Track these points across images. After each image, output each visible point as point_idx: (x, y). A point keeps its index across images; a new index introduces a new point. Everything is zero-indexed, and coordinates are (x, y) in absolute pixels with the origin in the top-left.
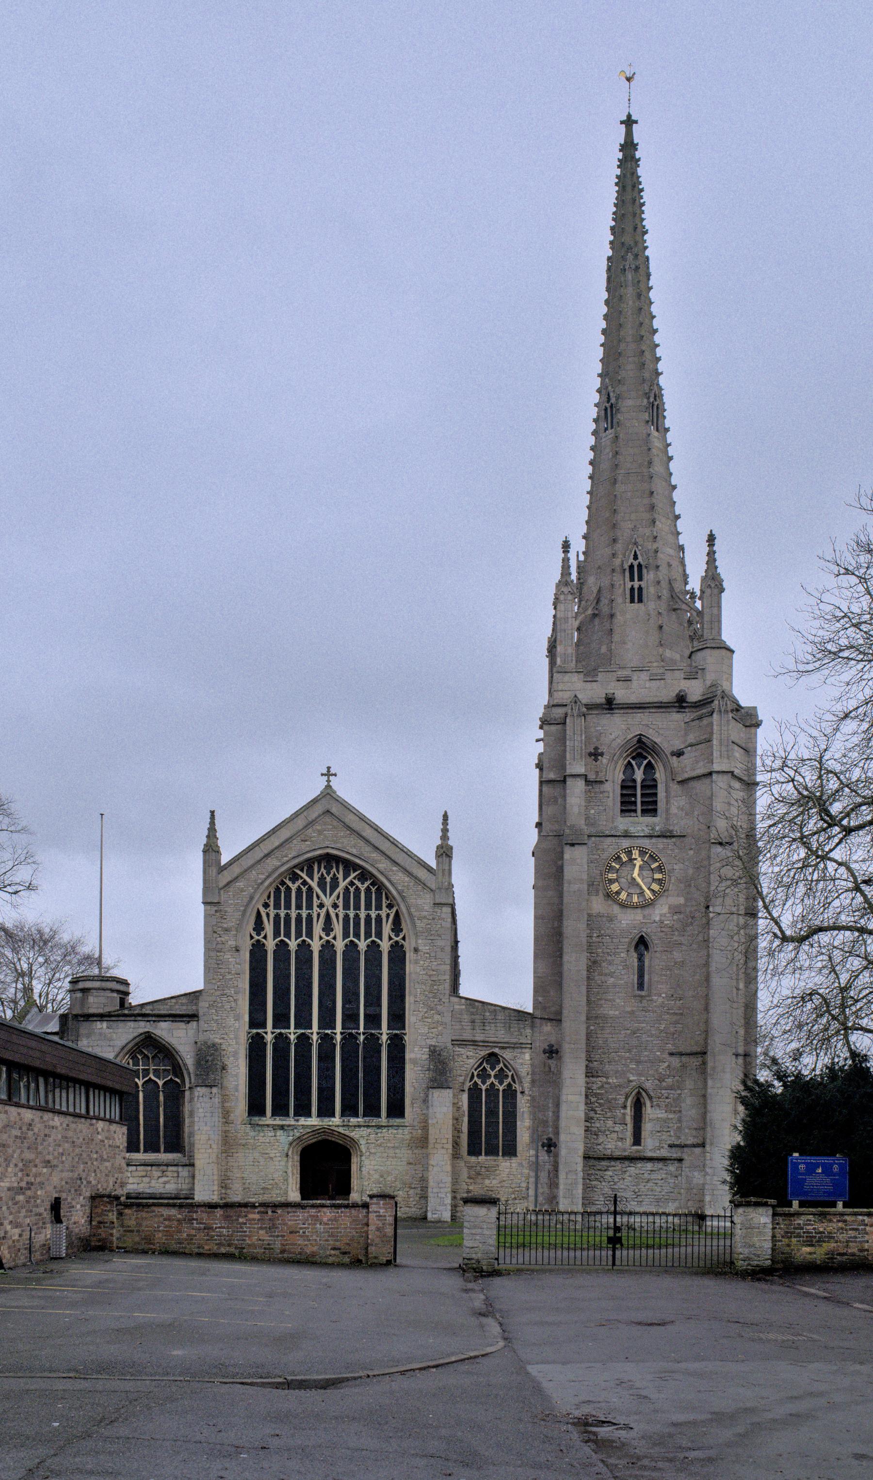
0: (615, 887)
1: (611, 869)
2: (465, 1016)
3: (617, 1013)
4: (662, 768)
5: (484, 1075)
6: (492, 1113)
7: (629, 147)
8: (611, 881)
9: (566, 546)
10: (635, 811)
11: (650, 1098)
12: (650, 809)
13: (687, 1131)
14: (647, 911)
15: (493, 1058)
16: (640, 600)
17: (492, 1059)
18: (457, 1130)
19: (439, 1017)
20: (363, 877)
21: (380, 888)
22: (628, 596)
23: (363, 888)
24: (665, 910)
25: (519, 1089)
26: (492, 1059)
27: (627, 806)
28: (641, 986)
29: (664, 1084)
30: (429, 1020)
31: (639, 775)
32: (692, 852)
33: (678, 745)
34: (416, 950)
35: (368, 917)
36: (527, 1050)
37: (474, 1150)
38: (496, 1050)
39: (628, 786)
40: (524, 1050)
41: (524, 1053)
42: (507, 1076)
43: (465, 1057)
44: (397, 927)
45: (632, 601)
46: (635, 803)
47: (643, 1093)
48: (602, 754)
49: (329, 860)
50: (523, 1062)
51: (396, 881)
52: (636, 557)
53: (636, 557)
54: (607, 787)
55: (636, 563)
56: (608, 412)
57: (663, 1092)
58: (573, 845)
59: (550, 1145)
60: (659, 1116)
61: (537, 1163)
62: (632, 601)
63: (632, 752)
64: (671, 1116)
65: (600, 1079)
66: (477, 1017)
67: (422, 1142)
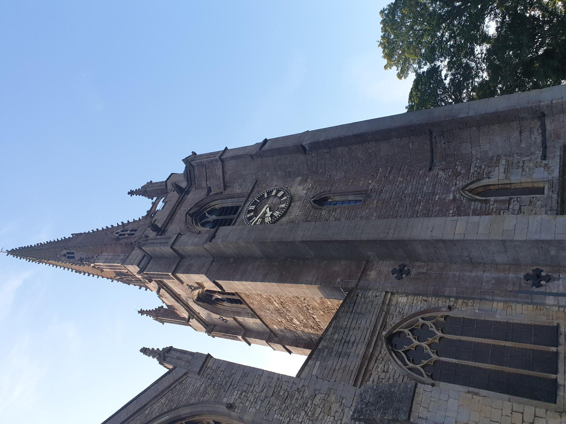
2: (330, 363)
6: (478, 353)
11: (478, 180)
13: (523, 145)
15: (395, 340)
19: (318, 397)
29: (463, 171)
30: (319, 410)
32: (268, 174)
36: (394, 299)
40: (394, 303)
41: (397, 303)
42: (423, 325)
47: (473, 186)
57: (472, 171)
66: (336, 348)
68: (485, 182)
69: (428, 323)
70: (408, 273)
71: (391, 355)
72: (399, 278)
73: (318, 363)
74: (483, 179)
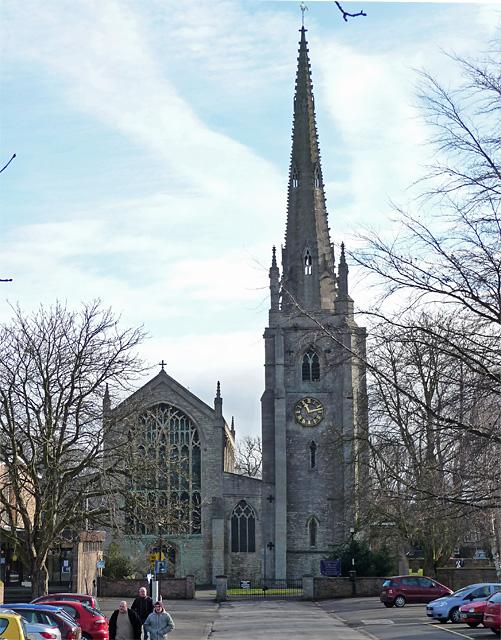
0: (300, 417)
5: (239, 512)
6: (243, 530)
7: (303, 43)
8: (298, 414)
9: (274, 250)
12: (316, 376)
18: (226, 539)
20: (179, 414)
21: (188, 419)
23: (180, 419)
26: (243, 503)
27: (306, 377)
31: (311, 362)
34: (205, 450)
35: (182, 434)
37: (235, 550)
39: (306, 366)
44: (196, 438)
49: (163, 406)
50: (258, 503)
51: (195, 416)
54: (296, 368)
59: (271, 546)
61: (265, 555)
67: (210, 546)
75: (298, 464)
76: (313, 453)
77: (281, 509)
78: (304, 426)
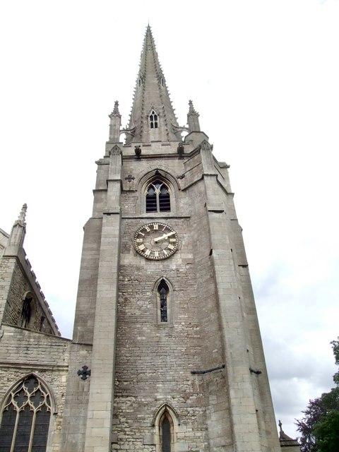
0: (142, 247)
1: (139, 236)
3: (144, 338)
4: (172, 186)
5: (20, 395)
8: (139, 244)
10: (156, 210)
11: (177, 416)
12: (166, 206)
14: (166, 263)
15: (32, 381)
16: (156, 127)
17: (30, 380)
22: (150, 125)
24: (180, 261)
25: (52, 411)
26: (30, 380)
27: (151, 206)
28: (164, 318)
29: (189, 401)
31: (158, 191)
33: (180, 174)
36: (64, 373)
38: (36, 373)
40: (61, 373)
43: (6, 379)
45: (152, 127)
46: (156, 206)
47: (171, 412)
48: (133, 179)
50: (59, 384)
52: (153, 113)
53: (153, 113)
54: (137, 194)
55: (153, 115)
56: (142, 79)
57: (189, 409)
58: (109, 214)
60: (187, 434)
62: (152, 127)
63: (153, 180)
64: (199, 434)
65: (129, 398)
68: (175, 421)
69: (45, 401)
70: (84, 379)
71: (18, 382)
72: (79, 373)
73: (12, 334)
74: (179, 421)
75: (138, 313)
76: (163, 305)
77: (101, 387)
78: (148, 259)
